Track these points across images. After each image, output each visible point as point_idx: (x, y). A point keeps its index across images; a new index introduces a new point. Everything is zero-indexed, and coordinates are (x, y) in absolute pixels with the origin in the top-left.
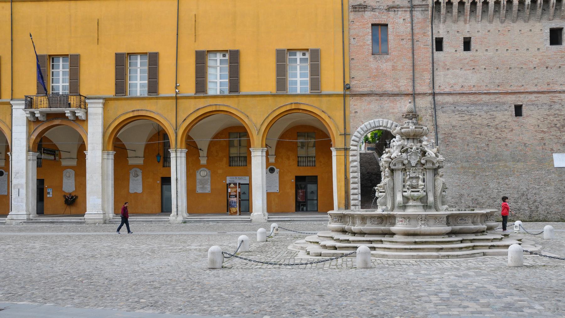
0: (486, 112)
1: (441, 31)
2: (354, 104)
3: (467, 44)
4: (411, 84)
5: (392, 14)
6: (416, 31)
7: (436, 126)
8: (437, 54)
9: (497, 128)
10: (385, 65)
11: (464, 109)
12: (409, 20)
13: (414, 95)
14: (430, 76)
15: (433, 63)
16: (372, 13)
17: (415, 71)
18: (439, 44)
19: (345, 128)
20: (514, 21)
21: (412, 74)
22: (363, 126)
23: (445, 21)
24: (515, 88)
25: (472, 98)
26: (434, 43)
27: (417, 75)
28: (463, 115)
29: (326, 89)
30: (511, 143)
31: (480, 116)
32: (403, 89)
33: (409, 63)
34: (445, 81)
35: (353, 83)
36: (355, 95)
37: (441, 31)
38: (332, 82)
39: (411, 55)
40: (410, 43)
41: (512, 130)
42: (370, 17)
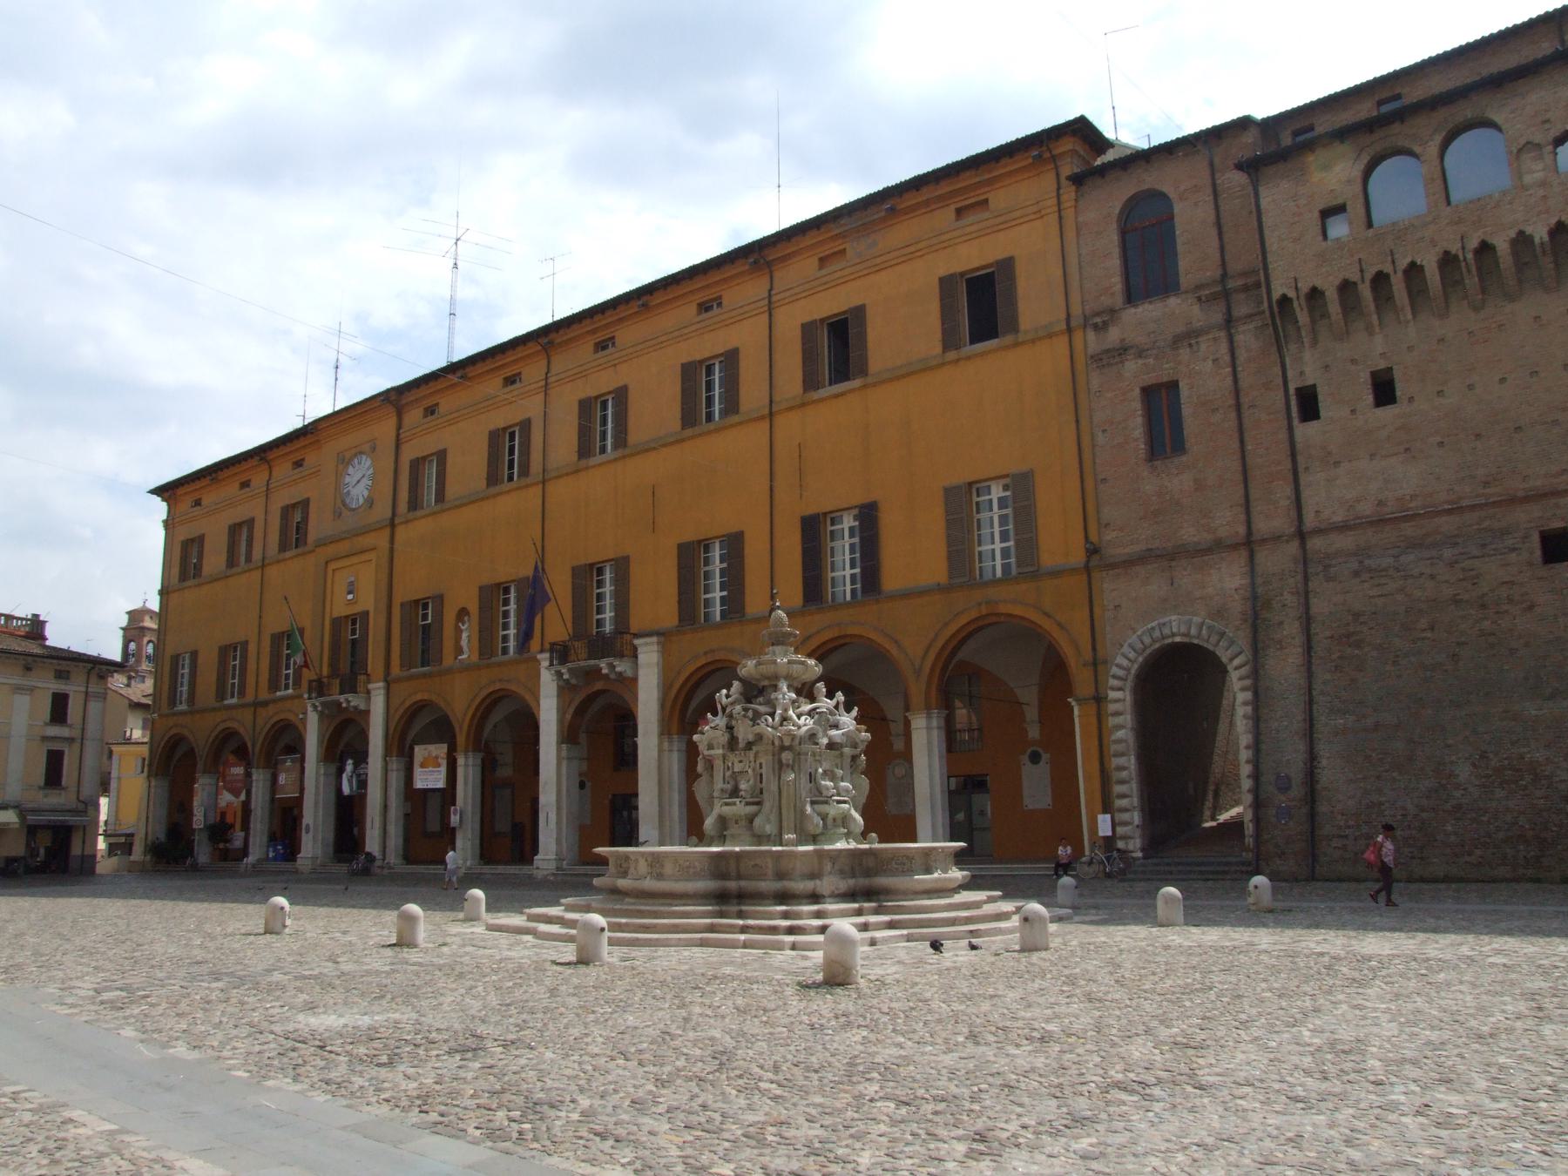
0: (1452, 565)
1: (1308, 367)
2: (1112, 589)
3: (1384, 390)
4: (1242, 517)
5: (1184, 353)
6: (1243, 384)
7: (1307, 620)
8: (1307, 432)
9: (1483, 606)
10: (1177, 480)
11: (1387, 561)
12: (1227, 358)
13: (1249, 544)
14: (1289, 490)
15: (1293, 455)
16: (1140, 361)
17: (1250, 485)
18: (1308, 405)
19: (1094, 649)
20: (1511, 298)
21: (1242, 492)
22: (1133, 639)
23: (1314, 342)
24: (1539, 483)
25: (1409, 529)
26: (1293, 402)
27: (1255, 493)
28: (1383, 581)
29: (1050, 557)
30: (1527, 645)
31: (1432, 577)
32: (1223, 533)
33: (1236, 465)
34: (1327, 496)
35: (1109, 536)
36: (1113, 566)
37: (1307, 370)
38: (1059, 543)
39: (1236, 445)
40: (1233, 415)
41: (1531, 607)
42: (1134, 373)
